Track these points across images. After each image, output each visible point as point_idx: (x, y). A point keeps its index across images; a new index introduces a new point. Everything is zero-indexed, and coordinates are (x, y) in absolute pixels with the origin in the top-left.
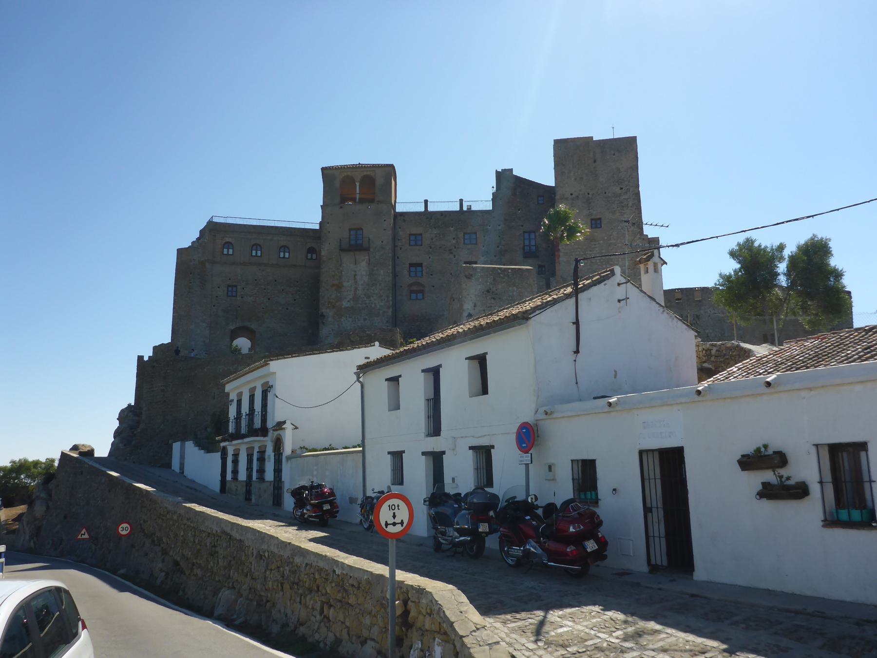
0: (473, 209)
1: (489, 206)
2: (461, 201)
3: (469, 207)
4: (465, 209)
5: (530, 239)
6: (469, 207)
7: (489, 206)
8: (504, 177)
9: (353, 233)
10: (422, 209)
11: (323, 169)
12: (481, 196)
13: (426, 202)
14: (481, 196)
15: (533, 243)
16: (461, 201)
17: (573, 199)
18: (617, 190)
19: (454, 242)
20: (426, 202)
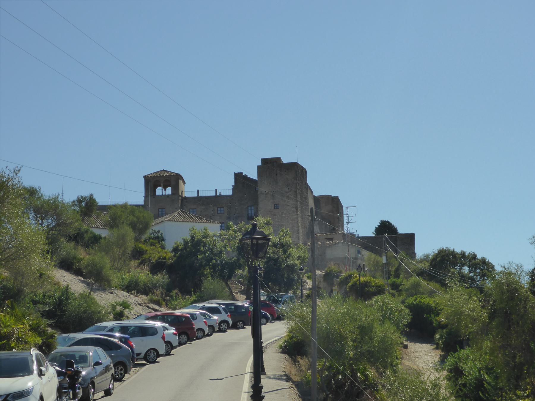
0: (222, 194)
1: (230, 193)
2: (216, 190)
3: (220, 194)
4: (218, 194)
5: (251, 210)
6: (220, 194)
7: (230, 193)
8: (239, 178)
9: (160, 210)
10: (196, 195)
11: (145, 177)
12: (226, 187)
13: (198, 191)
14: (226, 187)
15: (253, 212)
16: (216, 190)
17: (266, 194)
18: (287, 190)
19: (212, 212)
20: (198, 191)
